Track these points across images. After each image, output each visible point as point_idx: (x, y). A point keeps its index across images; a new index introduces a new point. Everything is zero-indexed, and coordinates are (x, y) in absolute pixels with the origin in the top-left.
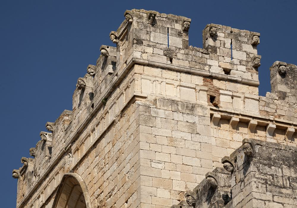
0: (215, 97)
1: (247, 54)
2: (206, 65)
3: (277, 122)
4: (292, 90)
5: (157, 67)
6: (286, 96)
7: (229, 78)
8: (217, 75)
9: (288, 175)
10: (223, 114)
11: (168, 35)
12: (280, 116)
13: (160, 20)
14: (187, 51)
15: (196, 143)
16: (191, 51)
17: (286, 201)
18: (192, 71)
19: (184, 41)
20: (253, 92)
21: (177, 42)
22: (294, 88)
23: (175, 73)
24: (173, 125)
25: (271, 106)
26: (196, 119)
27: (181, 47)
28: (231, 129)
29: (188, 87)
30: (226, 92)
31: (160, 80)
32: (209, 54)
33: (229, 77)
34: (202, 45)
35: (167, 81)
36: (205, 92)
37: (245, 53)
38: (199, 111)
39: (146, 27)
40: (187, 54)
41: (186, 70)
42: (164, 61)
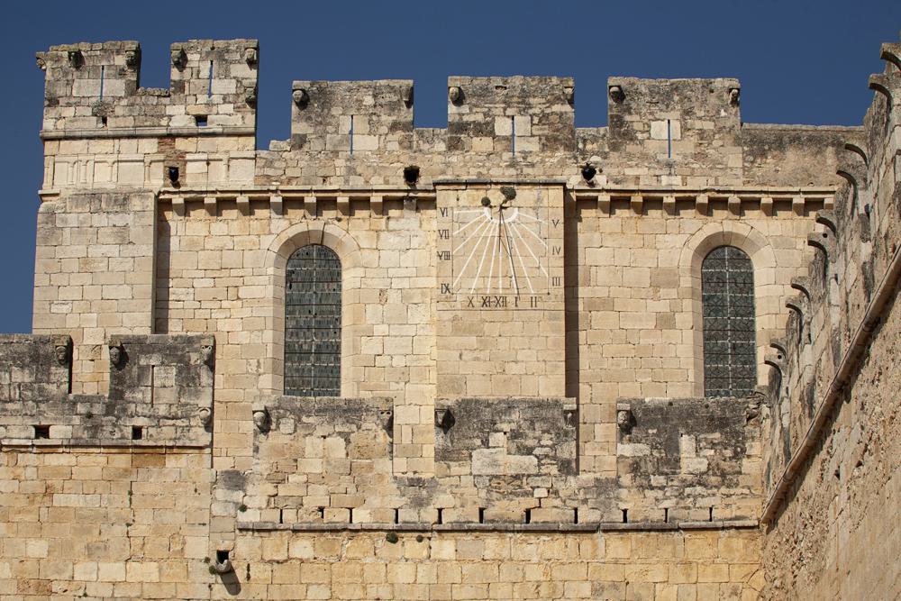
0: (177, 169)
1: (238, 81)
2: (162, 116)
3: (283, 191)
4: (318, 128)
5: (81, 138)
6: (305, 142)
7: (207, 131)
8: (180, 132)
9: (19, 380)
10: (188, 196)
11: (102, 79)
12: (290, 180)
13: (90, 57)
14: (132, 99)
15: (126, 260)
16: (138, 98)
17: (11, 420)
18: (138, 133)
19: (128, 84)
20: (244, 146)
21: (116, 87)
22: (321, 123)
23: (110, 142)
24: (89, 237)
25: (276, 164)
26: (129, 219)
27: (123, 94)
28: (208, 217)
29: (132, 161)
30: (196, 157)
31: (84, 158)
32: (169, 96)
33: (201, 129)
34: (164, 81)
35: (98, 158)
36: (161, 164)
37: (234, 81)
38: (136, 204)
39: (66, 74)
40: (132, 105)
41: (126, 133)
42: (92, 125)
